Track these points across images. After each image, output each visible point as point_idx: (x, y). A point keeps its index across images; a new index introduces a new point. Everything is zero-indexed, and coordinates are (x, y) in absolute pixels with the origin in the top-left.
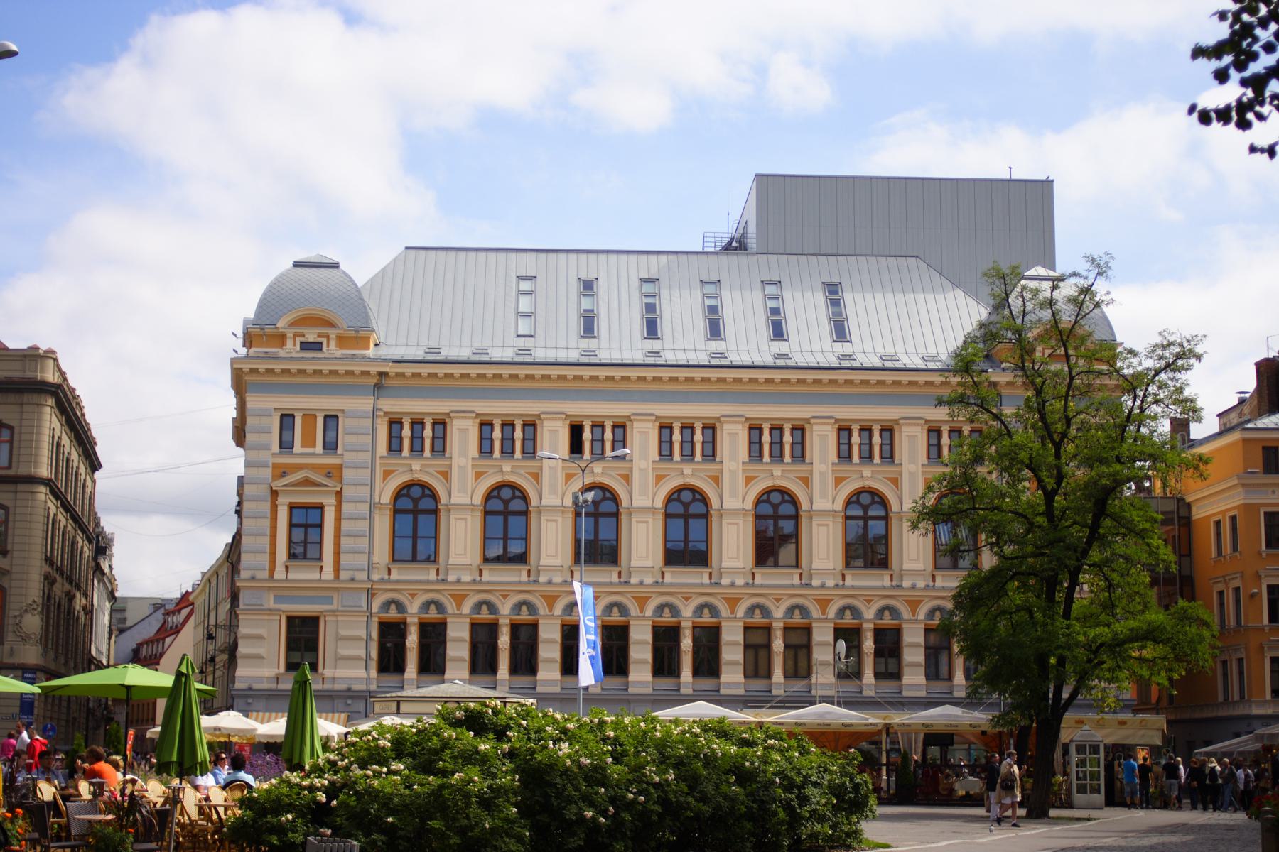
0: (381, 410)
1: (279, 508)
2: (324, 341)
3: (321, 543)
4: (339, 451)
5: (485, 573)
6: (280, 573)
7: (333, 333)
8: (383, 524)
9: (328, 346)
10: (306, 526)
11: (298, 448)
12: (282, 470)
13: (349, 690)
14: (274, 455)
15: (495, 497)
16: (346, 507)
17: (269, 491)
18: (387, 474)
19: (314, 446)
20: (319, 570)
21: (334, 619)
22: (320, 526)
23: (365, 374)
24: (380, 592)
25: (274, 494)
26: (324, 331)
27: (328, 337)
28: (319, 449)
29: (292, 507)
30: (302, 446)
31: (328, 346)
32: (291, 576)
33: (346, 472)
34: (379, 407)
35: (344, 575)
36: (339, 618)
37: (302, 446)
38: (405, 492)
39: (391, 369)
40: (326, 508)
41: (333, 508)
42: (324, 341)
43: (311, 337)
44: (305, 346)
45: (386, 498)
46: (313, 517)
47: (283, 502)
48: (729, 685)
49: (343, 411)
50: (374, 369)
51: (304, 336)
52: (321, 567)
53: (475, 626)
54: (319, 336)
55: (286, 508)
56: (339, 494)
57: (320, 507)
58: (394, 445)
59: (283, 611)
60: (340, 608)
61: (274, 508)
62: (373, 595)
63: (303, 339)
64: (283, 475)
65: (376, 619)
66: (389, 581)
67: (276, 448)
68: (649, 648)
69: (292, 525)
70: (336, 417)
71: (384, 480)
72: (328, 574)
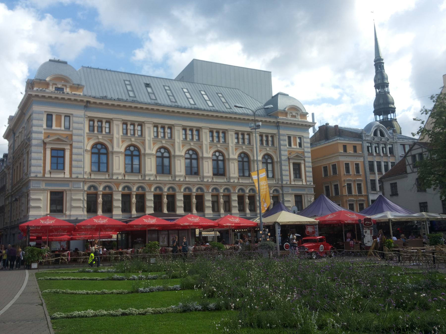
0: (87, 115)
1: (47, 149)
2: (65, 88)
3: (64, 164)
4: (71, 129)
5: (126, 176)
6: (47, 175)
7: (68, 85)
8: (87, 158)
10: (57, 157)
11: (54, 127)
12: (48, 135)
13: (77, 219)
14: (44, 129)
16: (74, 151)
17: (42, 142)
19: (60, 126)
21: (70, 192)
22: (64, 157)
23: (82, 101)
24: (88, 183)
25: (45, 144)
28: (63, 128)
29: (52, 149)
30: (56, 126)
31: (66, 90)
32: (52, 176)
33: (74, 138)
34: (86, 114)
35: (74, 176)
36: (72, 192)
37: (56, 126)
39: (92, 100)
40: (66, 150)
41: (69, 150)
42: (65, 88)
44: (57, 89)
45: (89, 148)
46: (60, 154)
47: (49, 147)
48: (208, 214)
49: (72, 114)
50: (85, 99)
52: (65, 173)
54: (63, 85)
55: (50, 149)
56: (71, 145)
57: (64, 150)
58: (92, 129)
59: (49, 189)
60: (72, 188)
61: (45, 150)
63: (56, 86)
64: (48, 137)
65: (86, 192)
66: (90, 179)
67: (45, 126)
69: (52, 157)
70: (69, 117)
72: (67, 175)
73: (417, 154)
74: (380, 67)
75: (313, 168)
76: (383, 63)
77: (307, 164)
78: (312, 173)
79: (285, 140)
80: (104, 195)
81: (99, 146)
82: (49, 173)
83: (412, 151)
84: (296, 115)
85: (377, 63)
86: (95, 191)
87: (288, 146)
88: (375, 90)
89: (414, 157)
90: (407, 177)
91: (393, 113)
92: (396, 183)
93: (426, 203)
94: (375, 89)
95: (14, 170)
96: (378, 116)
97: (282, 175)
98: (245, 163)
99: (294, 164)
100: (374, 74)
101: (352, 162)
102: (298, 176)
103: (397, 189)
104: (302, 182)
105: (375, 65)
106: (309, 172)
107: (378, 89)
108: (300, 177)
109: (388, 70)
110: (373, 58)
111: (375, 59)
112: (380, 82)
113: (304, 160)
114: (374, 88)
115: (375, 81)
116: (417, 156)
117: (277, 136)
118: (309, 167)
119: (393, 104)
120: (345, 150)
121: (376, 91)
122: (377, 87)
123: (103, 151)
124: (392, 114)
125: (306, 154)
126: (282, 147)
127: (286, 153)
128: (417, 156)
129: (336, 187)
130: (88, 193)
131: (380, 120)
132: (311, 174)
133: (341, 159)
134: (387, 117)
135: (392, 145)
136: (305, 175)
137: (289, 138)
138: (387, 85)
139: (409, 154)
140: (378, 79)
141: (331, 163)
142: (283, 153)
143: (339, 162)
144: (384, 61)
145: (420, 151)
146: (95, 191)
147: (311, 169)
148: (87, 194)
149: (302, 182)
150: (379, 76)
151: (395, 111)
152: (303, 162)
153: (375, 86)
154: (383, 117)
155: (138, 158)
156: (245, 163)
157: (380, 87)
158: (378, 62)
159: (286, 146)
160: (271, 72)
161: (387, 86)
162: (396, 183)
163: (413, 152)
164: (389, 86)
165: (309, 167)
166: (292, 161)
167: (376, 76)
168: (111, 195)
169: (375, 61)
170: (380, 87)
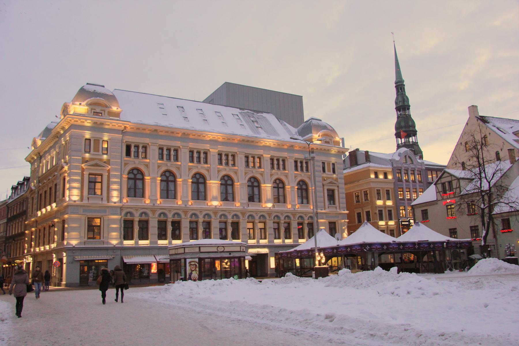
2: (103, 112)
3: (101, 189)
9: (104, 114)
15: (163, 175)
18: (126, 164)
19: (98, 151)
20: (101, 199)
24: (124, 209)
26: (103, 108)
27: (104, 111)
31: (104, 114)
38: (131, 171)
42: (103, 112)
43: (98, 110)
51: (95, 110)
52: (102, 199)
53: (159, 222)
54: (101, 110)
62: (122, 210)
68: (156, 229)
69: (90, 182)
71: (125, 166)
73: (446, 182)
74: (401, 89)
75: (347, 195)
76: (404, 85)
77: (340, 190)
78: (345, 200)
79: (319, 166)
80: (233, 223)
81: (135, 172)
82: (87, 199)
83: (442, 179)
84: (329, 141)
85: (398, 85)
86: (195, 219)
87: (322, 172)
88: (396, 112)
89: (443, 184)
90: (437, 204)
91: (415, 136)
92: (427, 210)
93: (456, 229)
94: (396, 111)
95: (41, 195)
96: (399, 139)
97: (316, 202)
98: (280, 189)
99: (328, 190)
100: (395, 96)
101: (383, 188)
102: (332, 202)
103: (427, 215)
104: (336, 209)
105: (396, 87)
106: (342, 198)
107: (400, 112)
108: (334, 204)
109: (408, 92)
110: (393, 79)
111: (396, 81)
112: (401, 104)
113: (338, 186)
114: (395, 110)
115: (396, 103)
116: (447, 184)
117: (312, 162)
118: (342, 193)
119: (415, 127)
120: (376, 176)
121: (397, 113)
122: (398, 109)
123: (139, 176)
124: (413, 137)
125: (339, 180)
126: (316, 173)
127: (321, 179)
128: (447, 184)
129: (368, 213)
130: (159, 220)
131: (402, 143)
132: (344, 201)
133: (372, 185)
134: (409, 140)
135: (420, 171)
136: (339, 201)
137: (323, 163)
138: (408, 107)
139: (439, 182)
140: (399, 102)
141: (363, 189)
142: (317, 179)
143: (370, 189)
144: (404, 83)
145: (449, 179)
146: (195, 219)
147: (344, 196)
148: (124, 221)
149: (336, 209)
150: (400, 99)
151: (416, 134)
152: (336, 188)
153: (396, 108)
154: (405, 140)
155: (173, 183)
156: (280, 189)
157: (401, 110)
158: (399, 84)
159: (321, 172)
160: (302, 96)
161: (409, 109)
162: (427, 210)
163: (443, 180)
164: (410, 109)
165: (342, 193)
166: (326, 188)
167: (397, 99)
168: (147, 222)
169: (396, 83)
170: (401, 110)
